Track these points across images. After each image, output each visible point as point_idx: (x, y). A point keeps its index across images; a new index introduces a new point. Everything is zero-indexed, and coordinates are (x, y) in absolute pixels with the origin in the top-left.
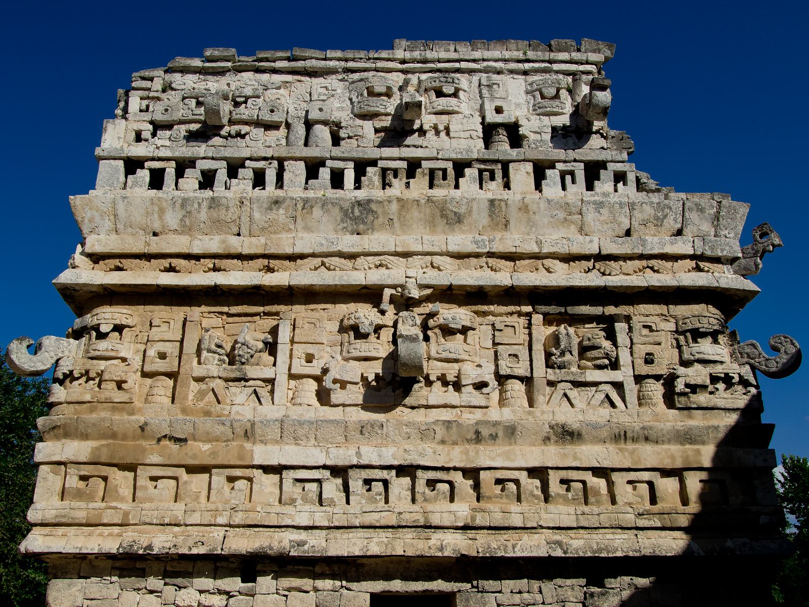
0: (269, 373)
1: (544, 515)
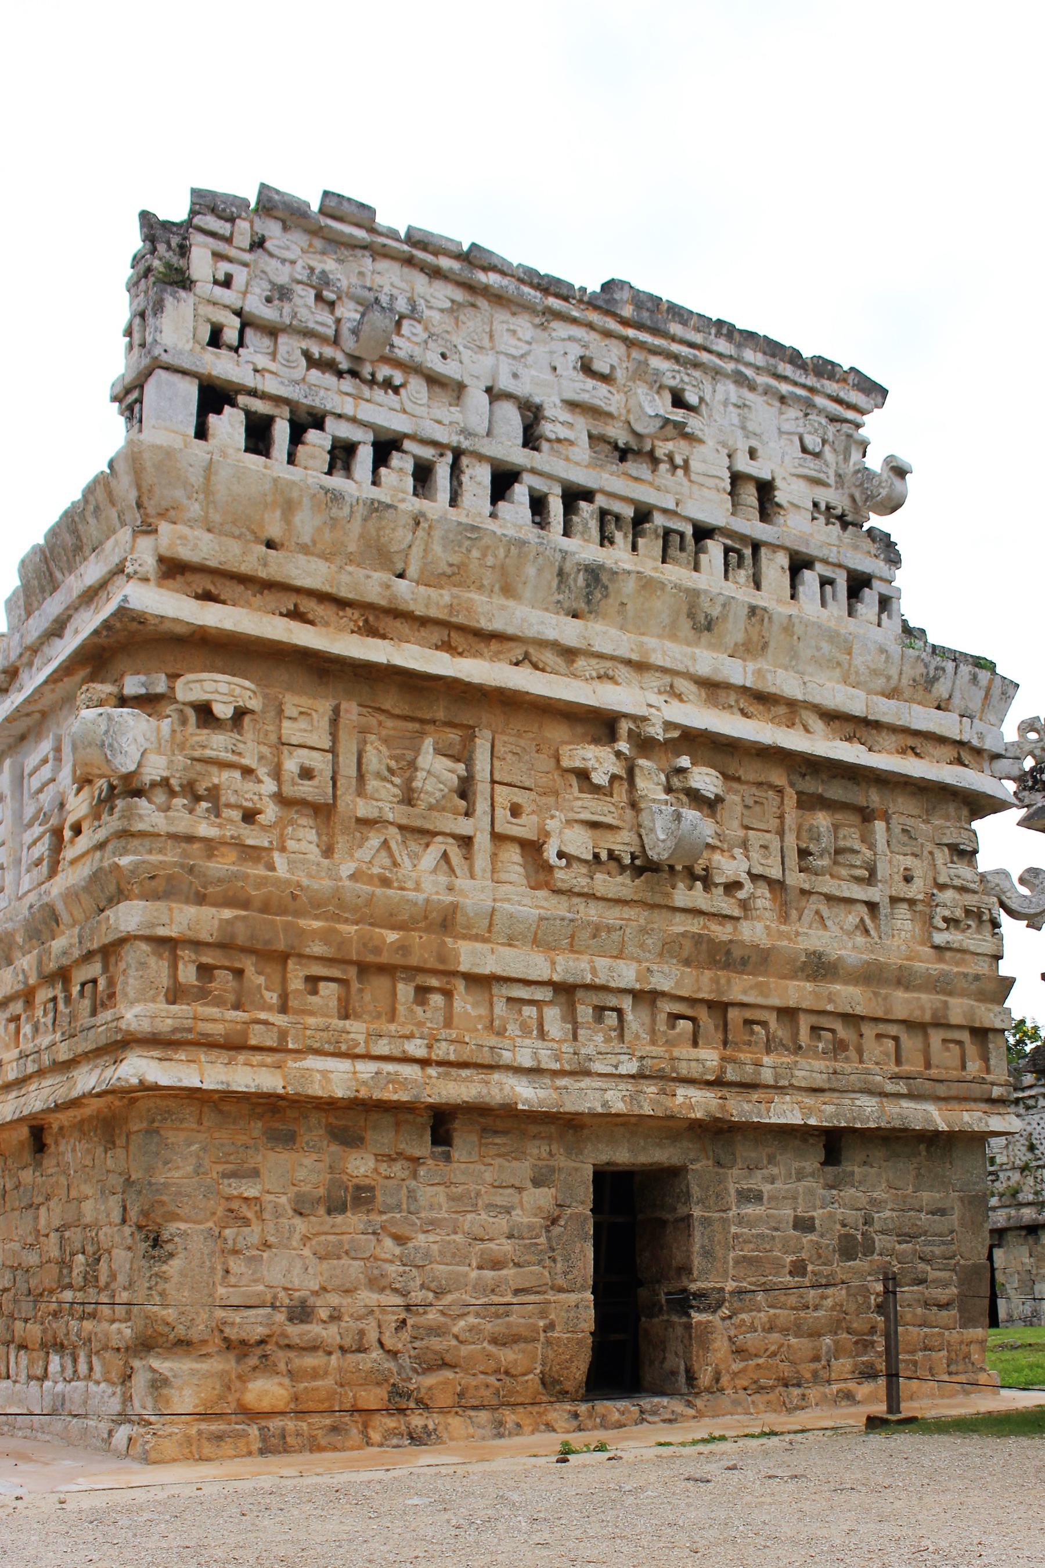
0: (464, 826)
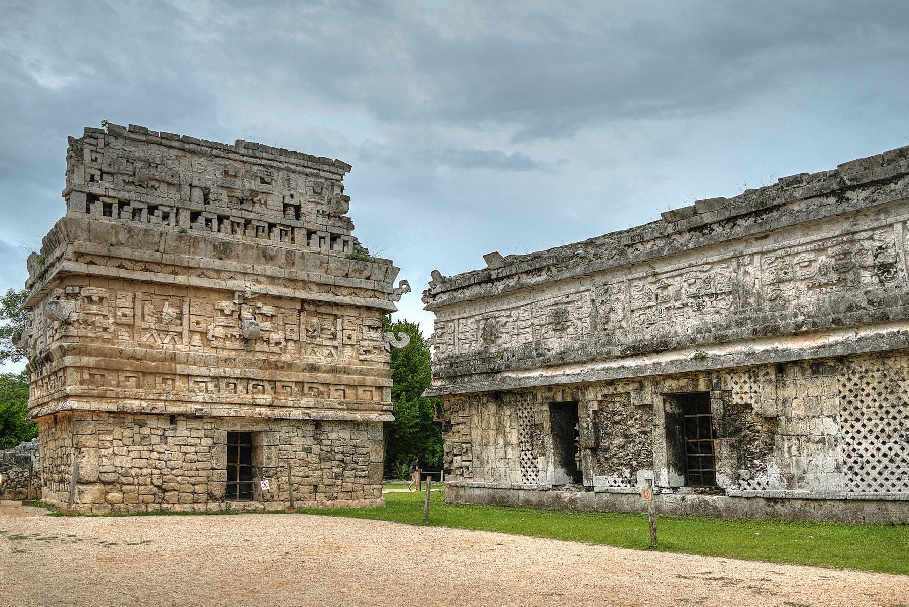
0: (179, 329)
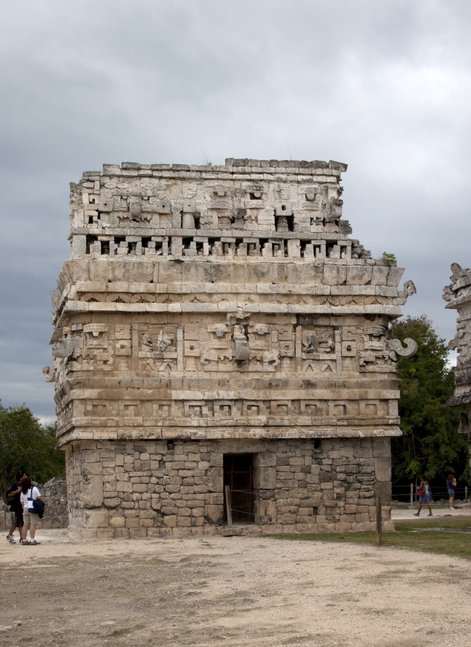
0: (174, 355)
1: (298, 421)
